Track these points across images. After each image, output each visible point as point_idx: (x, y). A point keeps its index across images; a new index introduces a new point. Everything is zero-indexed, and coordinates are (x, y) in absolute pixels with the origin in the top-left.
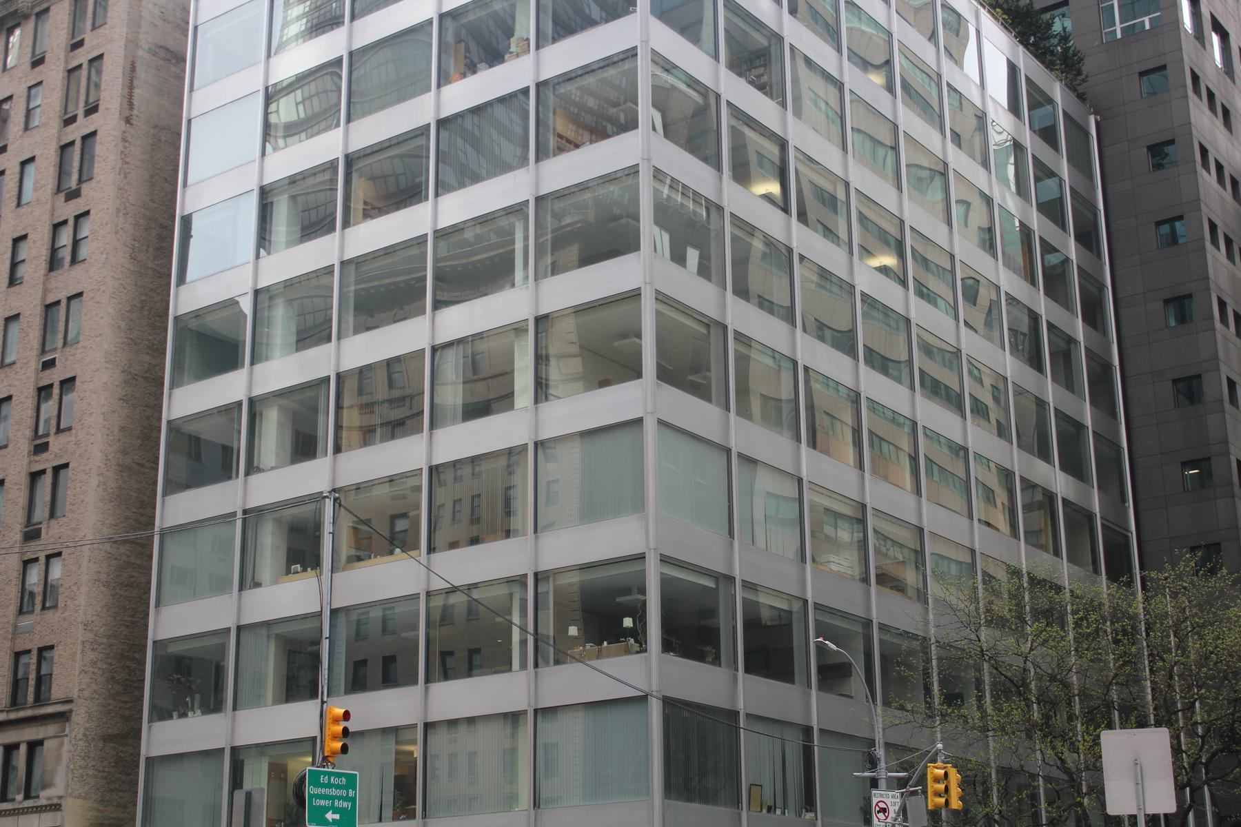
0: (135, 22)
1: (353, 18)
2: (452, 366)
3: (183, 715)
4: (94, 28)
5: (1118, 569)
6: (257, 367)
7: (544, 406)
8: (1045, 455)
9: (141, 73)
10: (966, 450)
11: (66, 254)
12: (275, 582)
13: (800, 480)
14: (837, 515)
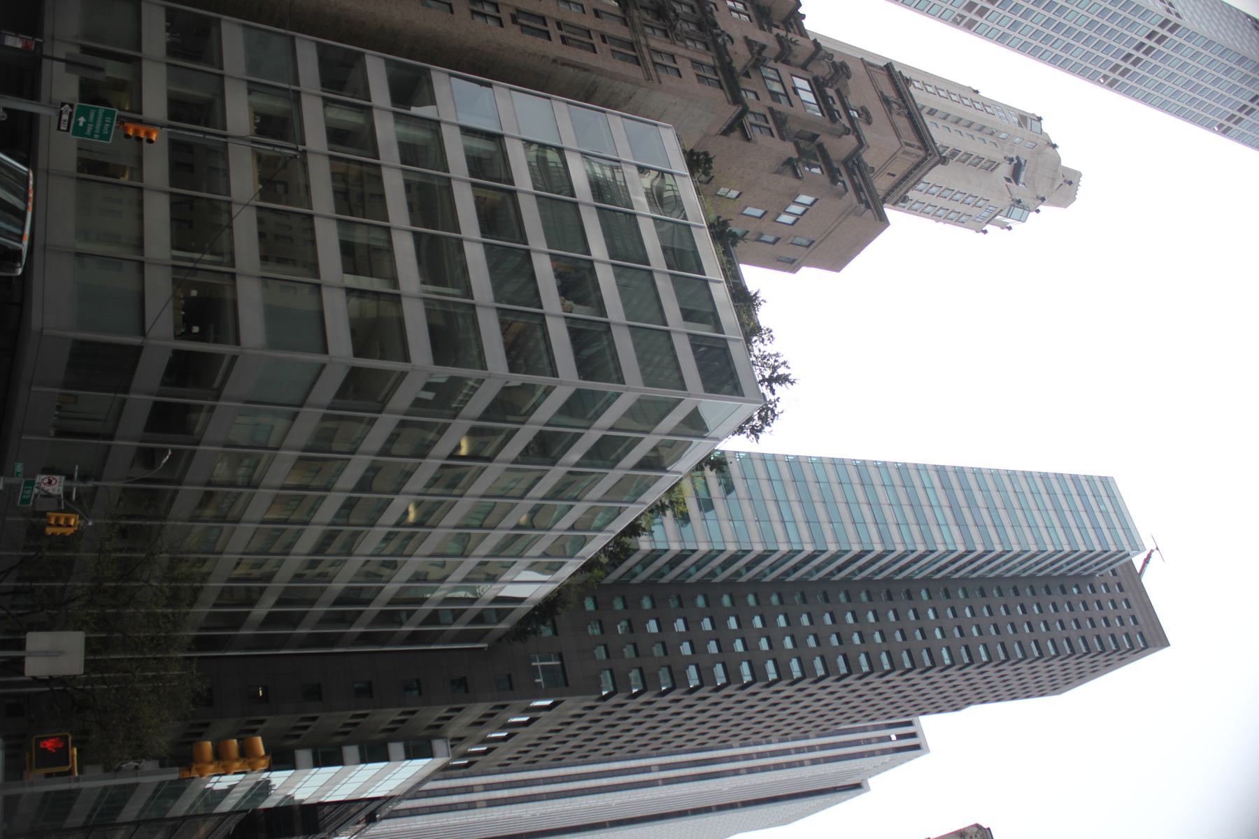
0: (613, 76)
1: (597, 208)
2: (376, 239)
3: (168, 29)
4: (613, 51)
5: (200, 643)
6: (391, 116)
7: (343, 293)
8: (279, 602)
9: (582, 74)
10: (287, 554)
11: (478, 8)
12: (250, 104)
13: (277, 449)
14: (255, 467)
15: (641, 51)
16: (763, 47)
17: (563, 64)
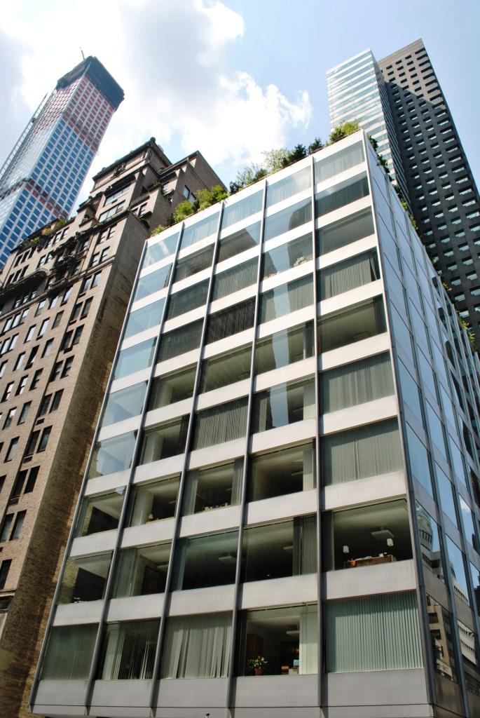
15: (92, 272)
16: (86, 216)
17: (102, 315)
